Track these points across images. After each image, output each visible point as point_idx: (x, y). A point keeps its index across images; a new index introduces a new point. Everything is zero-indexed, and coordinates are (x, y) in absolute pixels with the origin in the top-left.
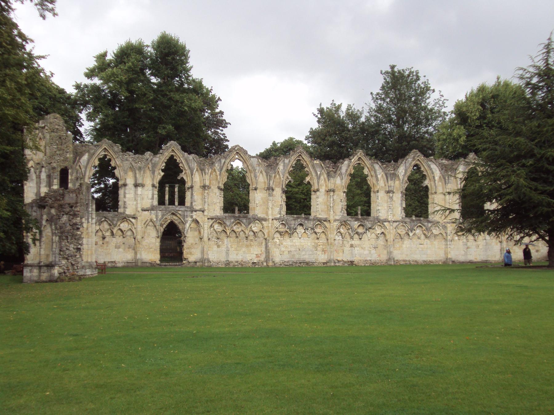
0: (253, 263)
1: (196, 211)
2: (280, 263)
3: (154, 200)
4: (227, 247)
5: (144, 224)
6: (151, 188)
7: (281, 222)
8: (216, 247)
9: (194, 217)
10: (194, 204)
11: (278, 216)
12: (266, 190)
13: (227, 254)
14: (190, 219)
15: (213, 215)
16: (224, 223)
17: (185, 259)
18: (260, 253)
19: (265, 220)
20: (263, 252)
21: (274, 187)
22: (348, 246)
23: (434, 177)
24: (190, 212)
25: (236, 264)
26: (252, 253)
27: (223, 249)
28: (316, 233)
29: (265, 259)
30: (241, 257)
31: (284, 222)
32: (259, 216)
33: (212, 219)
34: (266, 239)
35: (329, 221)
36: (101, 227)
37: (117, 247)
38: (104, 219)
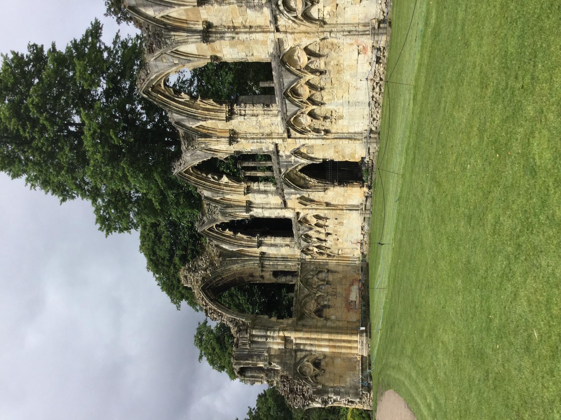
0: (378, 60)
2: (384, 5)
3: (268, 189)
4: (342, 105)
5: (306, 205)
6: (250, 195)
7: (282, 8)
8: (340, 122)
11: (267, 11)
13: (357, 104)
15: (280, 129)
18: (355, 47)
19: (279, 43)
20: (353, 42)
21: (200, 27)
24: (280, 158)
25: (377, 90)
27: (345, 111)
30: (364, 82)
32: (271, 50)
33: (288, 131)
36: (314, 236)
37: (341, 224)
38: (303, 236)
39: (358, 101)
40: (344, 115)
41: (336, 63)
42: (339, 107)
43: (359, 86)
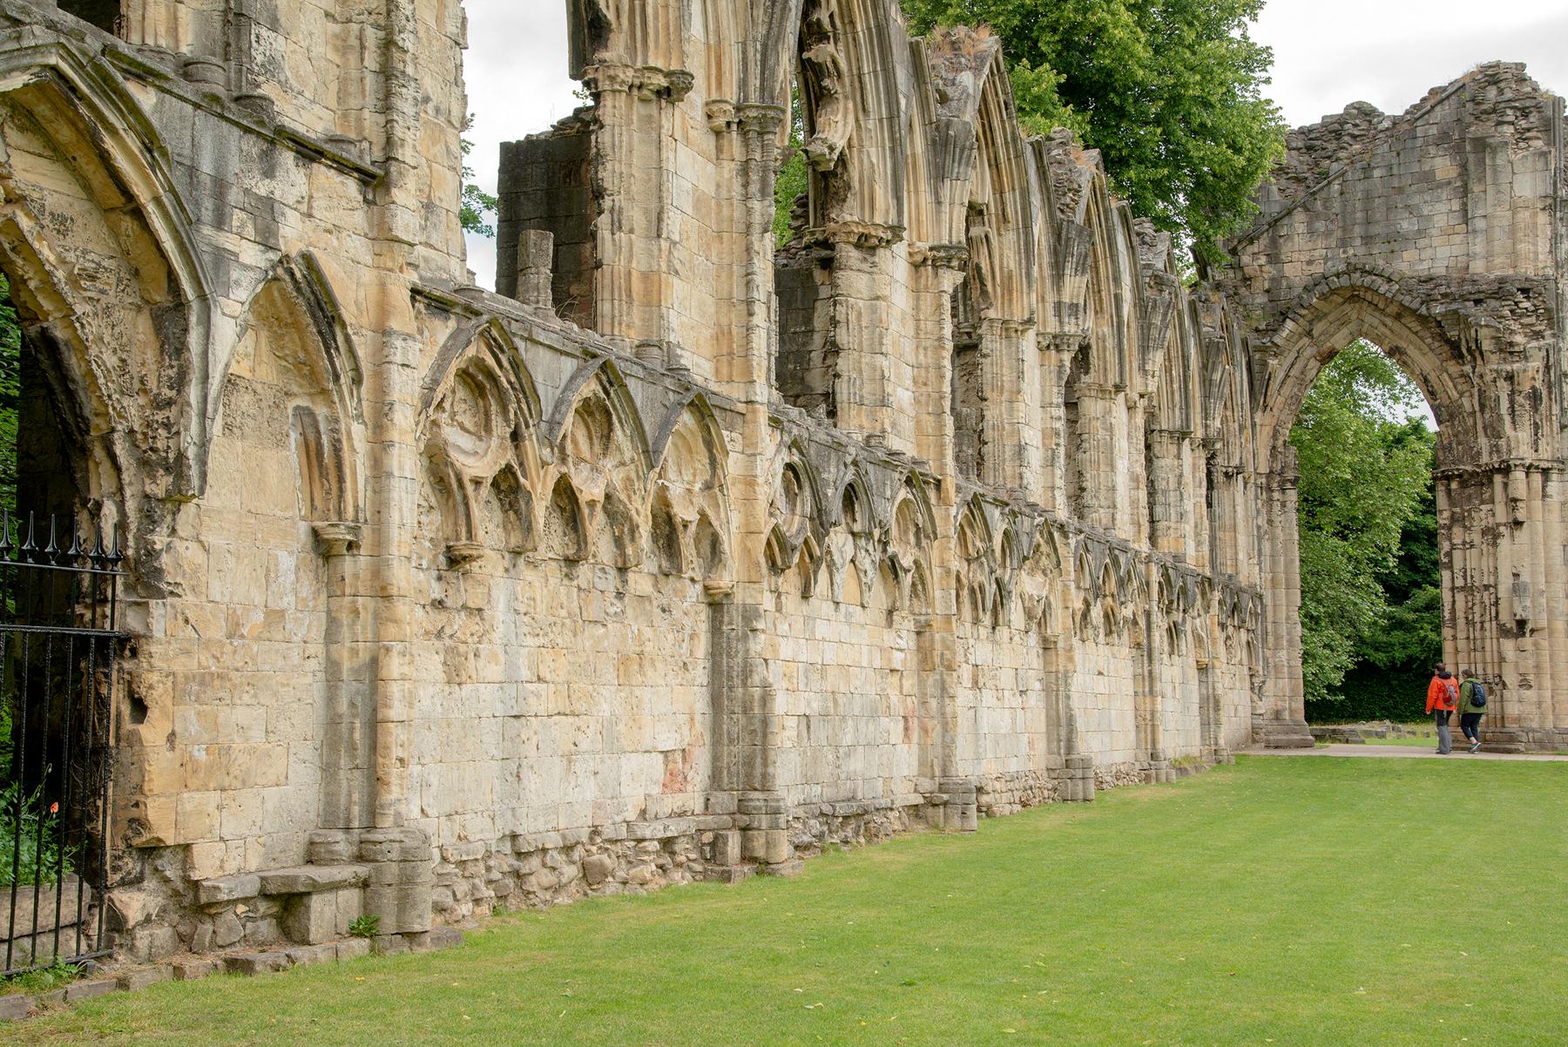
1: (309, 152)
8: (432, 664)
9: (293, 234)
10: (265, 44)
12: (718, 134)
14: (251, 254)
16: (527, 390)
17: (151, 851)
20: (699, 728)
22: (966, 672)
23: (1118, 299)
24: (253, 146)
26: (647, 743)
28: (892, 568)
29: (726, 800)
30: (590, 790)
31: (796, 458)
34: (716, 604)
35: (938, 484)
39: (525, 772)
40: (467, 689)
41: (649, 647)
42: (502, 658)
43: (578, 767)
